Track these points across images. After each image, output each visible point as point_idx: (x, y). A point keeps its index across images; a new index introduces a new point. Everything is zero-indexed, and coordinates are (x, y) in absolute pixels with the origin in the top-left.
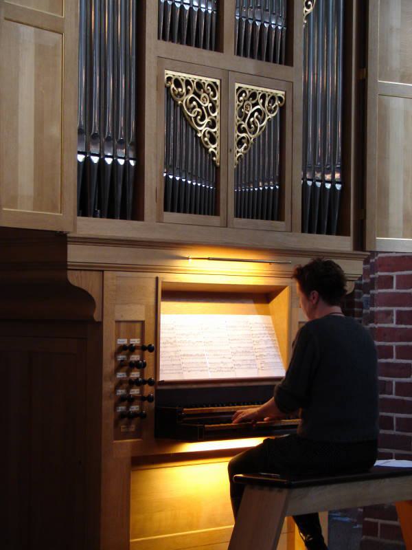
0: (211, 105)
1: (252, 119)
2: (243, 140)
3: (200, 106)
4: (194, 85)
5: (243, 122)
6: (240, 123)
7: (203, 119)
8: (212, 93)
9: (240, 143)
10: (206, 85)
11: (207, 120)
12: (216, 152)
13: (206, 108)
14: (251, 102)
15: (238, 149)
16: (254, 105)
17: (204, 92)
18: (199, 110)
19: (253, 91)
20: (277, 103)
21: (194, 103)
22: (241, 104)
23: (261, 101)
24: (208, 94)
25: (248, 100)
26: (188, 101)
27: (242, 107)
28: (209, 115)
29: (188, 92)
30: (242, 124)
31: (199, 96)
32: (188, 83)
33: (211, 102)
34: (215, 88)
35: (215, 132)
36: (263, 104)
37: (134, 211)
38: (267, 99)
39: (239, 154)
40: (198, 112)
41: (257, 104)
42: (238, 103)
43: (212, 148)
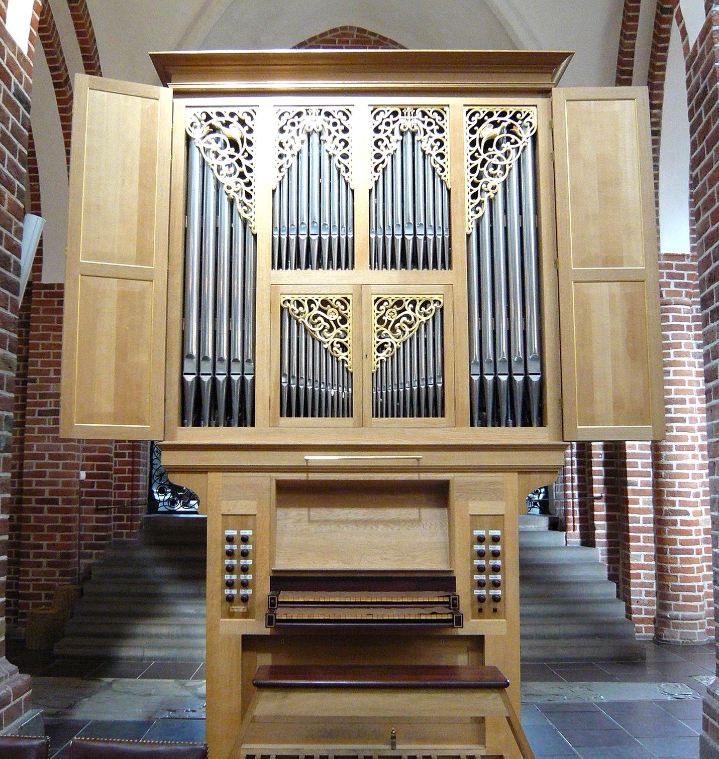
0: (340, 318)
1: (397, 325)
2: (385, 345)
3: (326, 320)
4: (318, 303)
5: (385, 329)
6: (379, 330)
7: (331, 330)
8: (343, 307)
9: (381, 348)
10: (334, 301)
11: (336, 331)
12: (347, 360)
13: (335, 321)
14: (396, 309)
15: (377, 354)
16: (399, 312)
17: (332, 307)
18: (327, 324)
19: (398, 299)
20: (433, 306)
21: (320, 318)
22: (382, 313)
23: (411, 306)
24: (337, 309)
25: (392, 307)
26: (311, 317)
27: (384, 315)
28: (338, 327)
29: (311, 310)
30: (383, 331)
31: (325, 312)
32: (310, 302)
33: (340, 314)
34: (346, 302)
35: (347, 342)
36: (413, 310)
37: (246, 418)
38: (419, 304)
39: (379, 359)
40: (325, 326)
41: (404, 310)
42: (377, 312)
43: (342, 356)
